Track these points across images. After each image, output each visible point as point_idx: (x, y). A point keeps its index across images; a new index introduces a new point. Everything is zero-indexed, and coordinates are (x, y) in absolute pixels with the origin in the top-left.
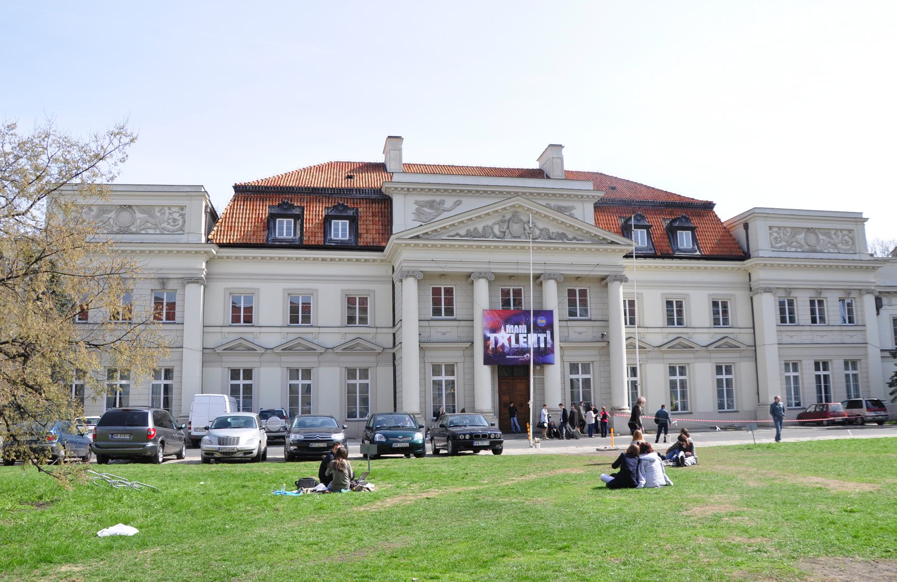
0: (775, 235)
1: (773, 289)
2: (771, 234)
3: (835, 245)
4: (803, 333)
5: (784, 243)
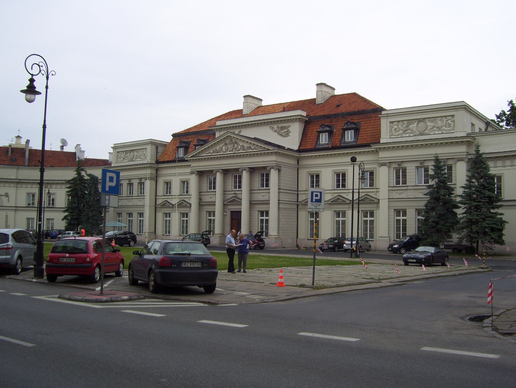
0: (395, 127)
4: (408, 191)
5: (401, 132)
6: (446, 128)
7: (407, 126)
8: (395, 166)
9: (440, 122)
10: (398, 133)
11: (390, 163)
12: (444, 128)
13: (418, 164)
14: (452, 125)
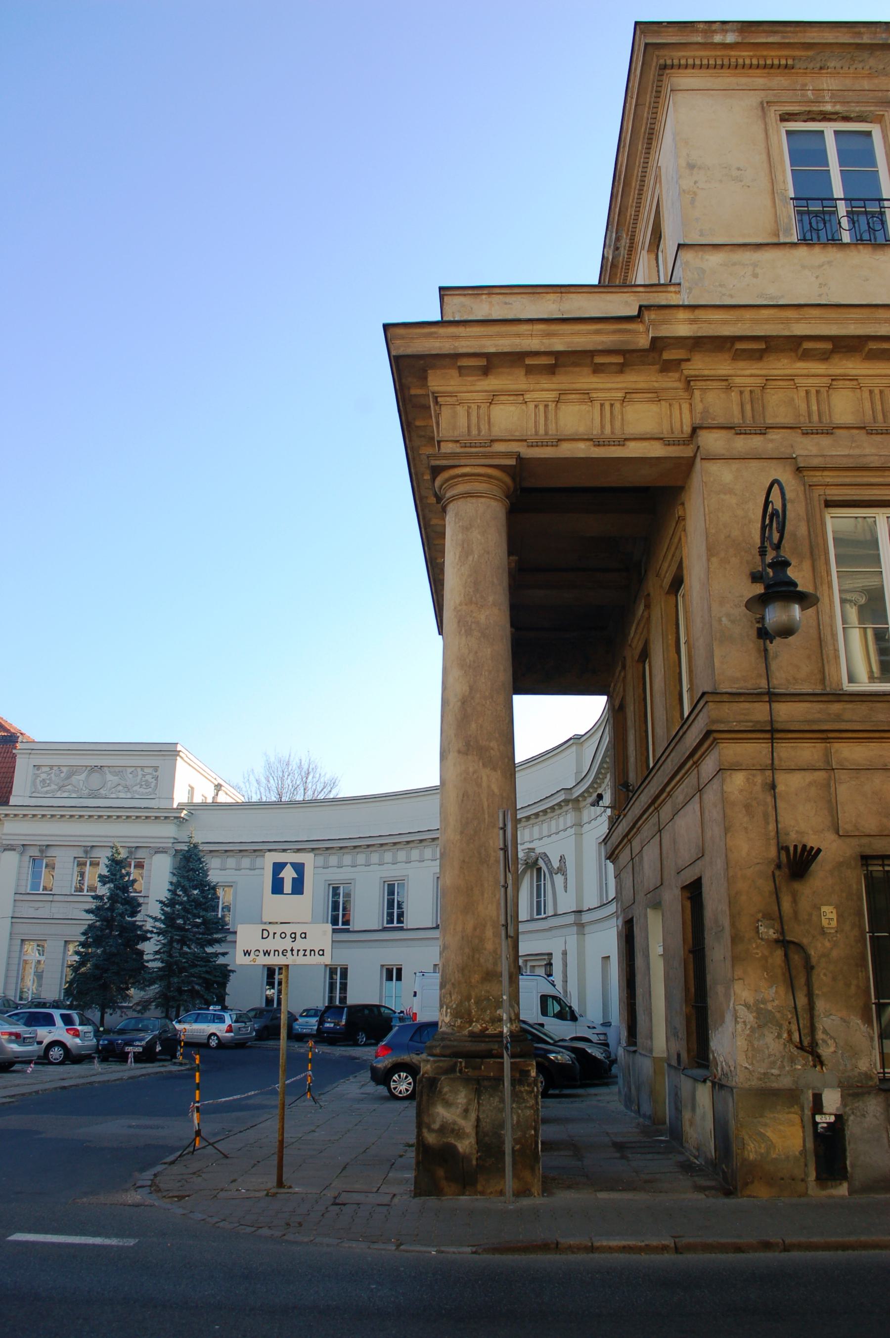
0: (44, 776)
1: (18, 845)
3: (127, 789)
5: (53, 787)
6: (142, 790)
7: (68, 777)
8: (35, 852)
9: (130, 776)
10: (48, 788)
11: (23, 845)
12: (135, 788)
13: (79, 853)
14: (153, 785)
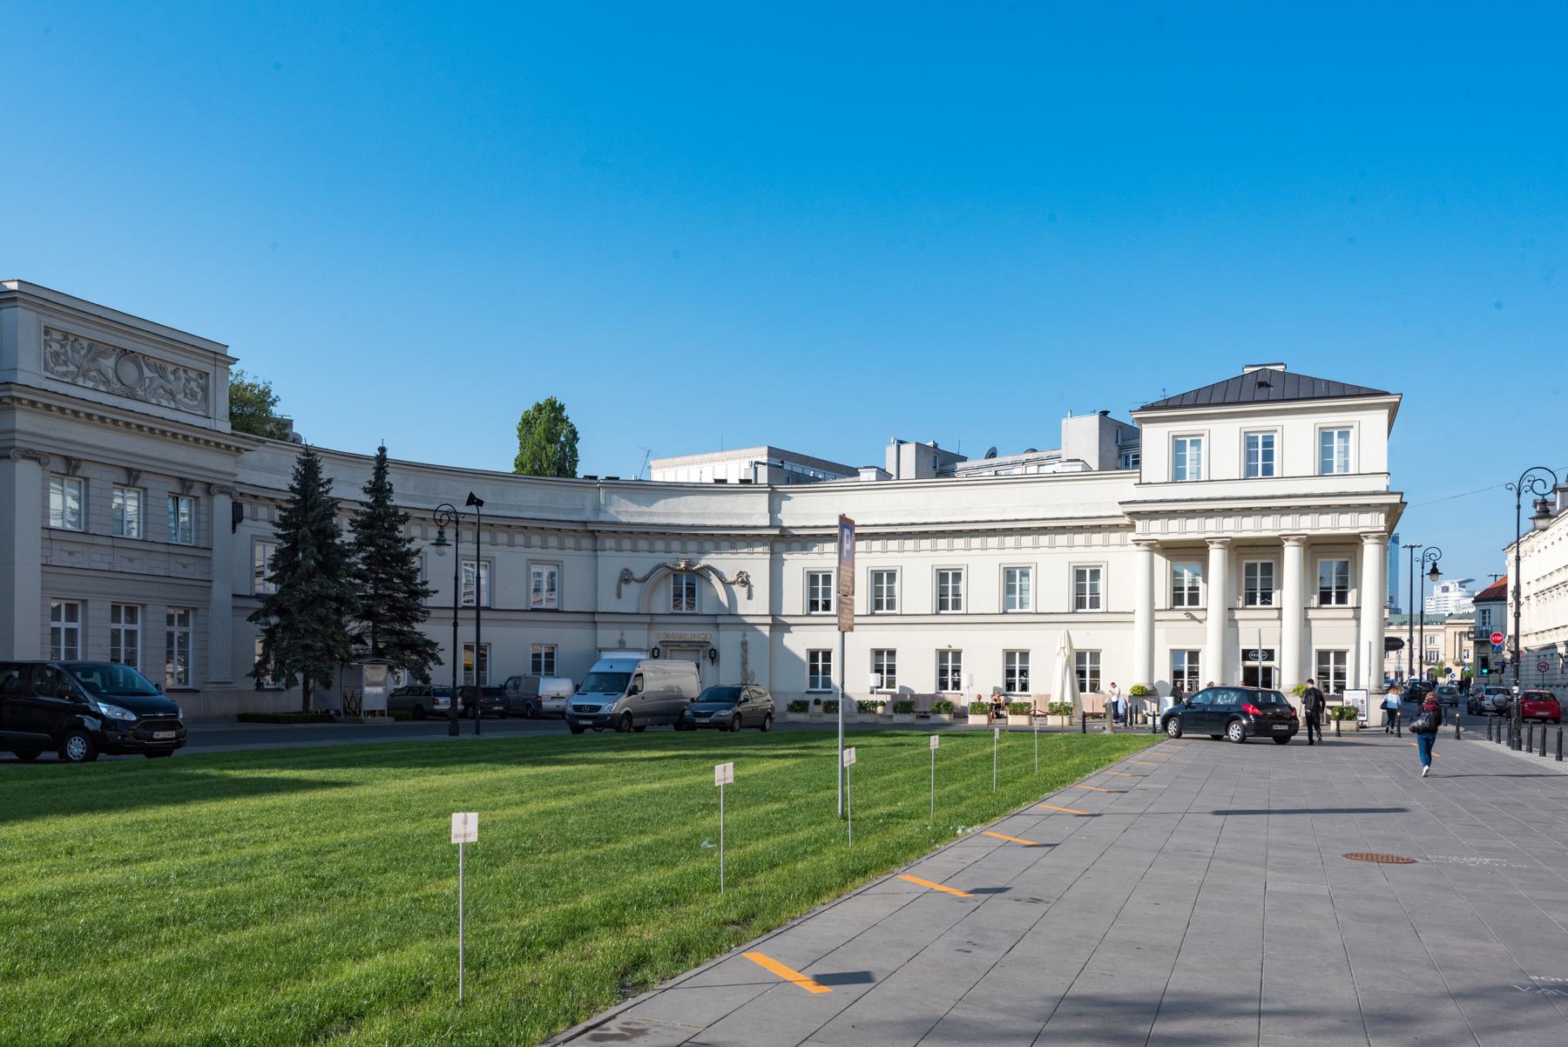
0: (56, 347)
2: (46, 344)
3: (172, 395)
5: (72, 368)
10: (64, 369)
